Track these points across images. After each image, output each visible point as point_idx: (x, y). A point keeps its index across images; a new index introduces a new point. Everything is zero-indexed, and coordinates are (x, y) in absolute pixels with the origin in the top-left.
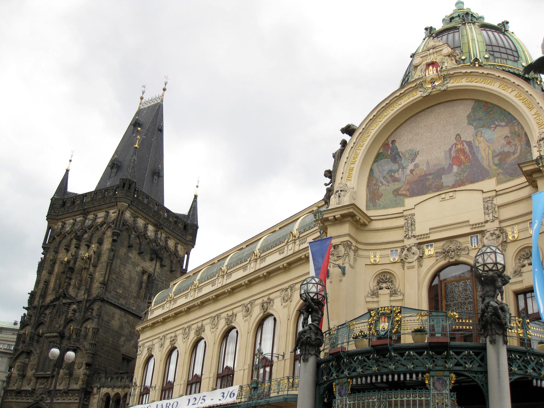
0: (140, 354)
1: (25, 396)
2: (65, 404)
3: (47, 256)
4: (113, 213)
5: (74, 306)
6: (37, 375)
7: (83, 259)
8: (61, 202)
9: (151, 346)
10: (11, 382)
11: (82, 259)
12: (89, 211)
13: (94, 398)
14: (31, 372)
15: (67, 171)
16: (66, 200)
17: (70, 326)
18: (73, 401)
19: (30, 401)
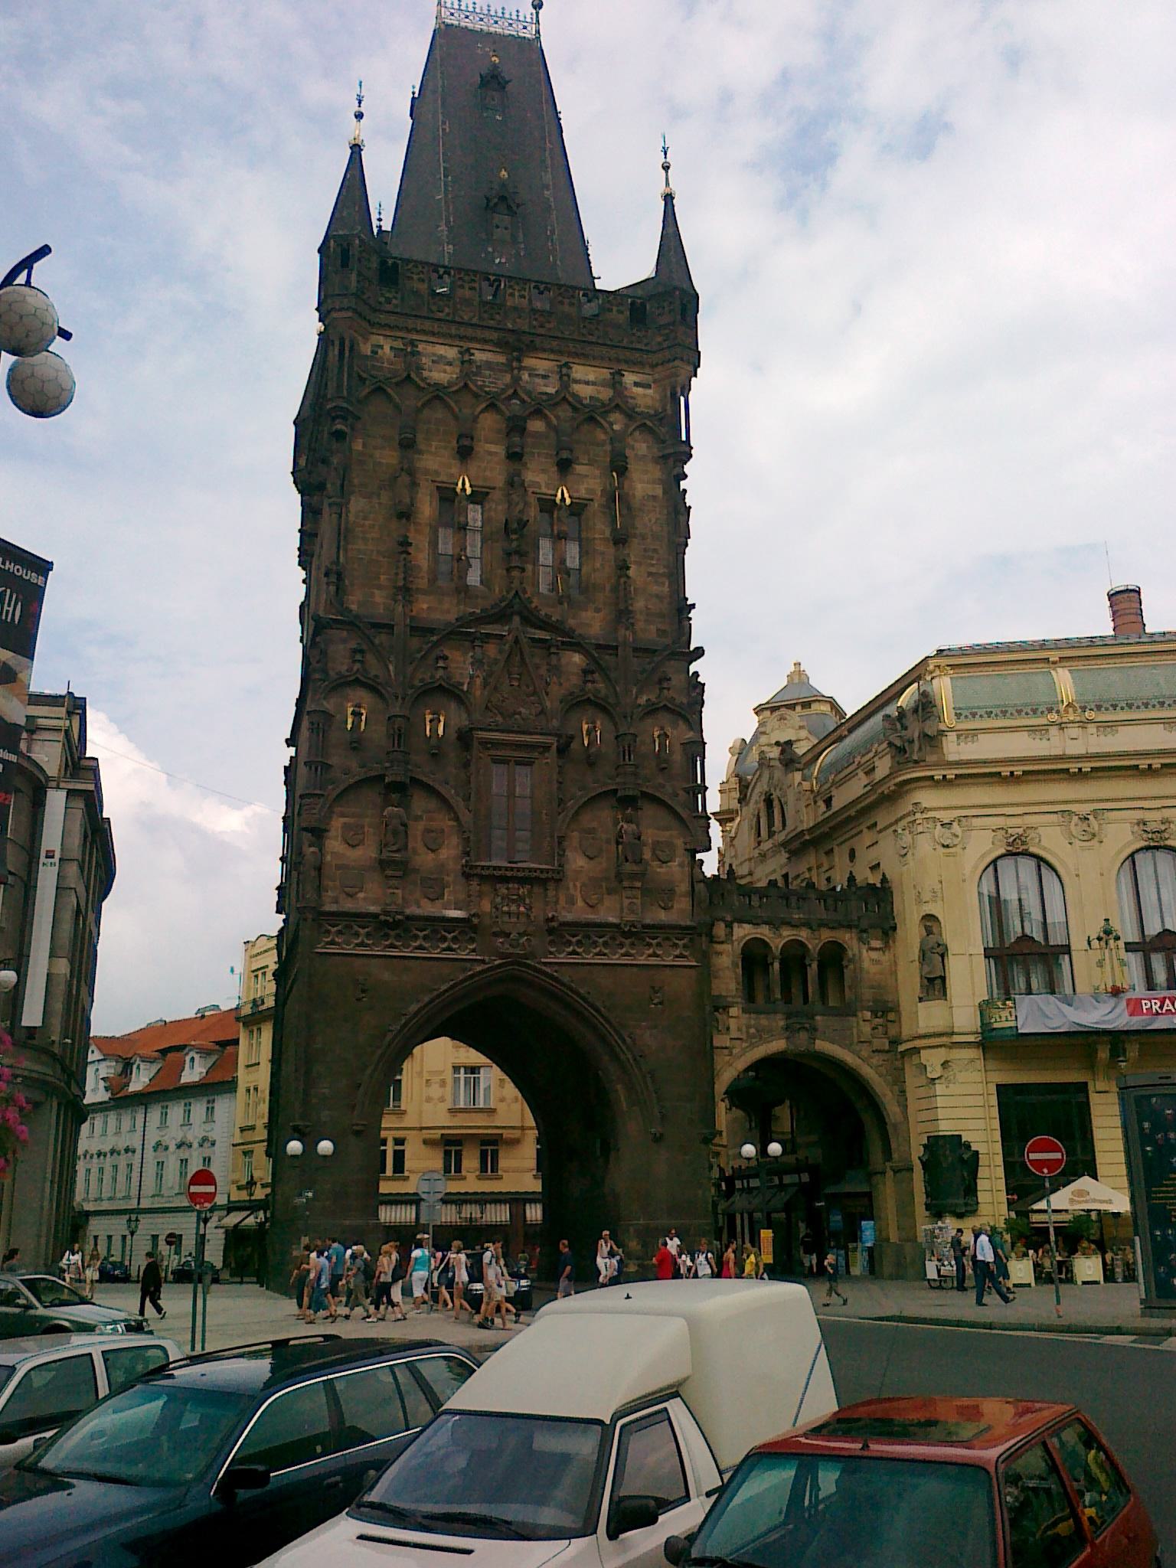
0: (955, 845)
1: (425, 938)
2: (635, 969)
3: (358, 446)
4: (636, 384)
5: (577, 658)
6: (483, 867)
7: (548, 506)
8: (374, 263)
9: (1020, 831)
10: (327, 883)
11: (539, 499)
12: (538, 341)
13: (720, 953)
14: (431, 856)
15: (356, 149)
16: (395, 265)
17: (594, 722)
18: (669, 961)
19: (463, 955)
